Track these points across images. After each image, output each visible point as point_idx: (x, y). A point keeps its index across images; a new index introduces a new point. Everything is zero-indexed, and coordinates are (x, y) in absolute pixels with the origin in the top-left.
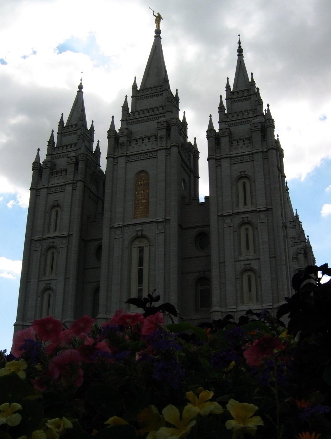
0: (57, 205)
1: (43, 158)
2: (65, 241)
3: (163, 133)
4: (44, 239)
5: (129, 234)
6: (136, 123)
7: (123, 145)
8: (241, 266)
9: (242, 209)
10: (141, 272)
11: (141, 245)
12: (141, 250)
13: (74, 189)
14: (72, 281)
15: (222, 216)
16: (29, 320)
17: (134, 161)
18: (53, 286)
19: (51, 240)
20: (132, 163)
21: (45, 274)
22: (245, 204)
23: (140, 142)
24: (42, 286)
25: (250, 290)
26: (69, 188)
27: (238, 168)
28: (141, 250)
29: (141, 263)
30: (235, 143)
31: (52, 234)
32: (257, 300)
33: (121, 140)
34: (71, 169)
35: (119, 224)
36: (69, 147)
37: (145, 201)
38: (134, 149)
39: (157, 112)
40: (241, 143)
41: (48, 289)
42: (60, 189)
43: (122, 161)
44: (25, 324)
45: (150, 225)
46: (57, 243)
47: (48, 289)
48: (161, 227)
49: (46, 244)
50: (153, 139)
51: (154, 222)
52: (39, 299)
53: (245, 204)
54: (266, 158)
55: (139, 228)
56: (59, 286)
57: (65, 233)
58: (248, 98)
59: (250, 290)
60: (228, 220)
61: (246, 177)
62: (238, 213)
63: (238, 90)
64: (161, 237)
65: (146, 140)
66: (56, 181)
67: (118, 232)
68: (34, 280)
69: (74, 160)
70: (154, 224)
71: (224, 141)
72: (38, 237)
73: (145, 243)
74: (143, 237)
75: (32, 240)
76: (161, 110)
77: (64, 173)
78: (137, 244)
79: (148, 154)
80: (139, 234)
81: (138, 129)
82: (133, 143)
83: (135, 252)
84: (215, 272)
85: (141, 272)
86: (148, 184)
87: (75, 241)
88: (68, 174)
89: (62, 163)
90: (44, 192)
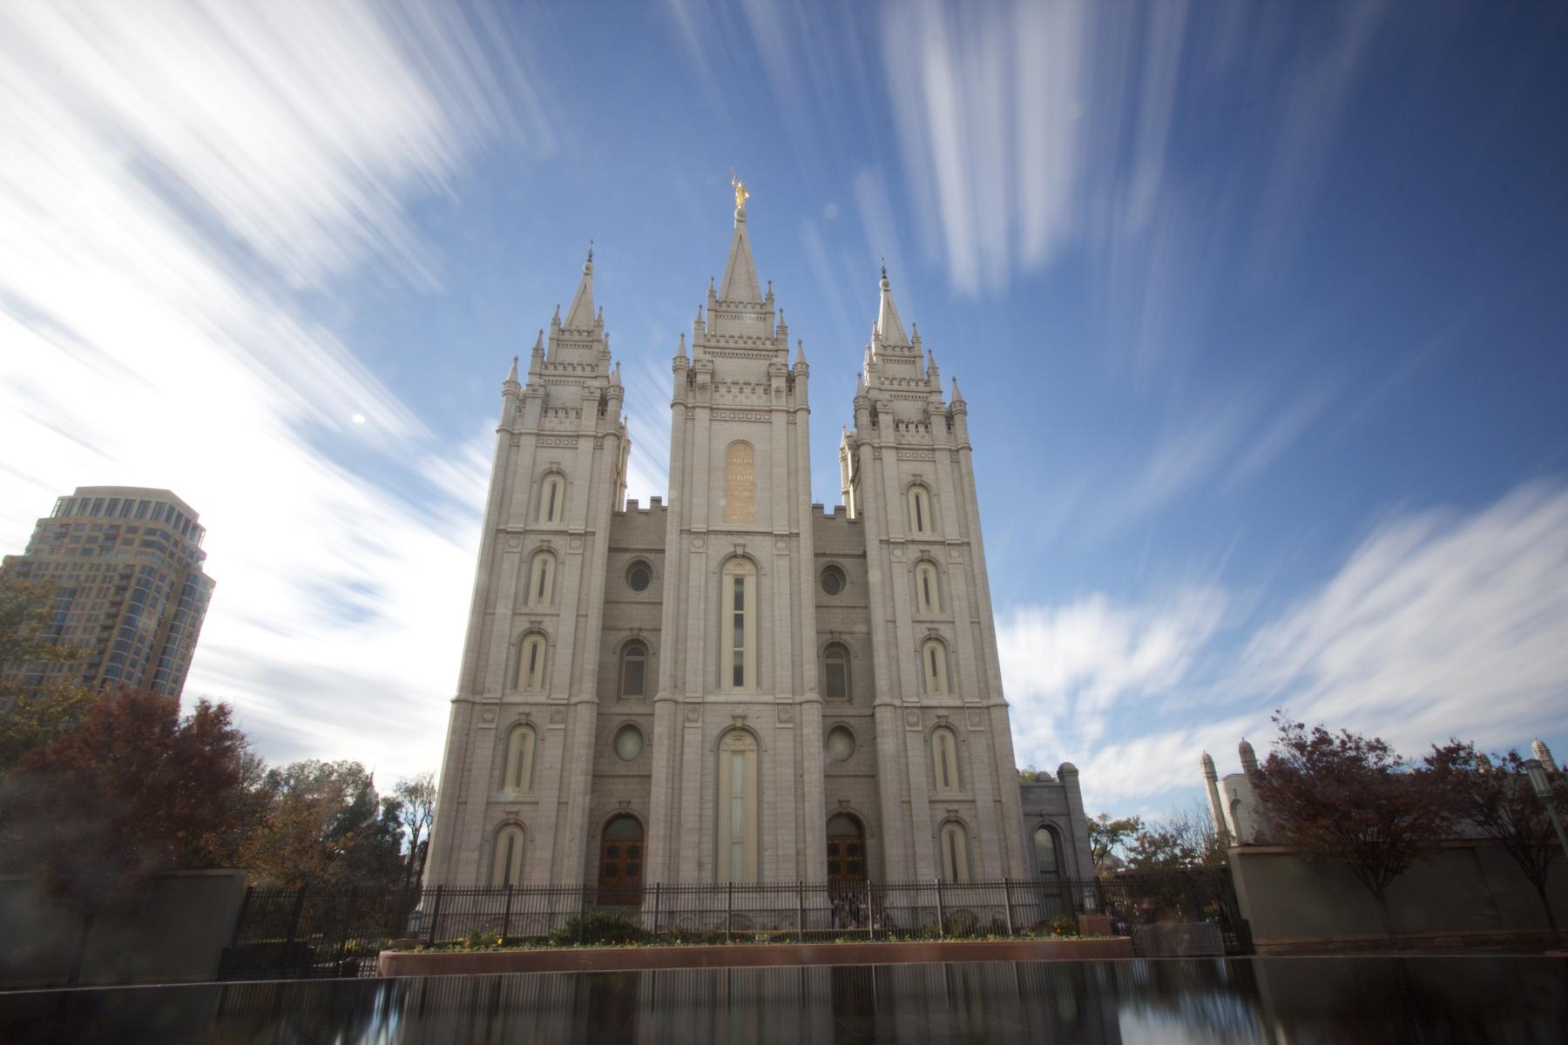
1: (524, 380)
2: (576, 543)
3: (779, 383)
4: (526, 532)
5: (722, 547)
6: (723, 355)
7: (703, 387)
8: (923, 631)
9: (917, 536)
10: (739, 621)
11: (740, 571)
12: (739, 582)
13: (599, 447)
14: (594, 622)
15: (888, 542)
18: (548, 625)
19: (544, 537)
21: (526, 602)
22: (920, 529)
24: (523, 624)
25: (935, 674)
26: (586, 446)
27: (909, 468)
28: (739, 582)
30: (902, 427)
31: (545, 525)
32: (950, 690)
33: (700, 379)
34: (591, 410)
35: (701, 527)
36: (579, 369)
37: (746, 494)
38: (725, 399)
40: (912, 427)
41: (536, 631)
43: (702, 415)
44: (478, 699)
46: (559, 543)
48: (781, 545)
49: (532, 542)
50: (760, 390)
51: (770, 534)
52: (513, 651)
53: (920, 529)
54: (955, 462)
55: (739, 540)
56: (562, 629)
57: (577, 526)
58: (913, 360)
59: (935, 674)
60: (898, 552)
61: (923, 485)
62: (913, 542)
63: (892, 343)
64: (784, 563)
65: (747, 390)
67: (698, 542)
68: (503, 609)
69: (598, 394)
71: (885, 420)
72: (516, 525)
73: (746, 569)
74: (745, 556)
75: (498, 531)
76: (768, 345)
77: (573, 414)
78: (733, 568)
80: (740, 551)
81: (728, 367)
82: (723, 390)
84: (879, 637)
86: (751, 465)
87: (600, 544)
89: (567, 394)
90: (528, 443)
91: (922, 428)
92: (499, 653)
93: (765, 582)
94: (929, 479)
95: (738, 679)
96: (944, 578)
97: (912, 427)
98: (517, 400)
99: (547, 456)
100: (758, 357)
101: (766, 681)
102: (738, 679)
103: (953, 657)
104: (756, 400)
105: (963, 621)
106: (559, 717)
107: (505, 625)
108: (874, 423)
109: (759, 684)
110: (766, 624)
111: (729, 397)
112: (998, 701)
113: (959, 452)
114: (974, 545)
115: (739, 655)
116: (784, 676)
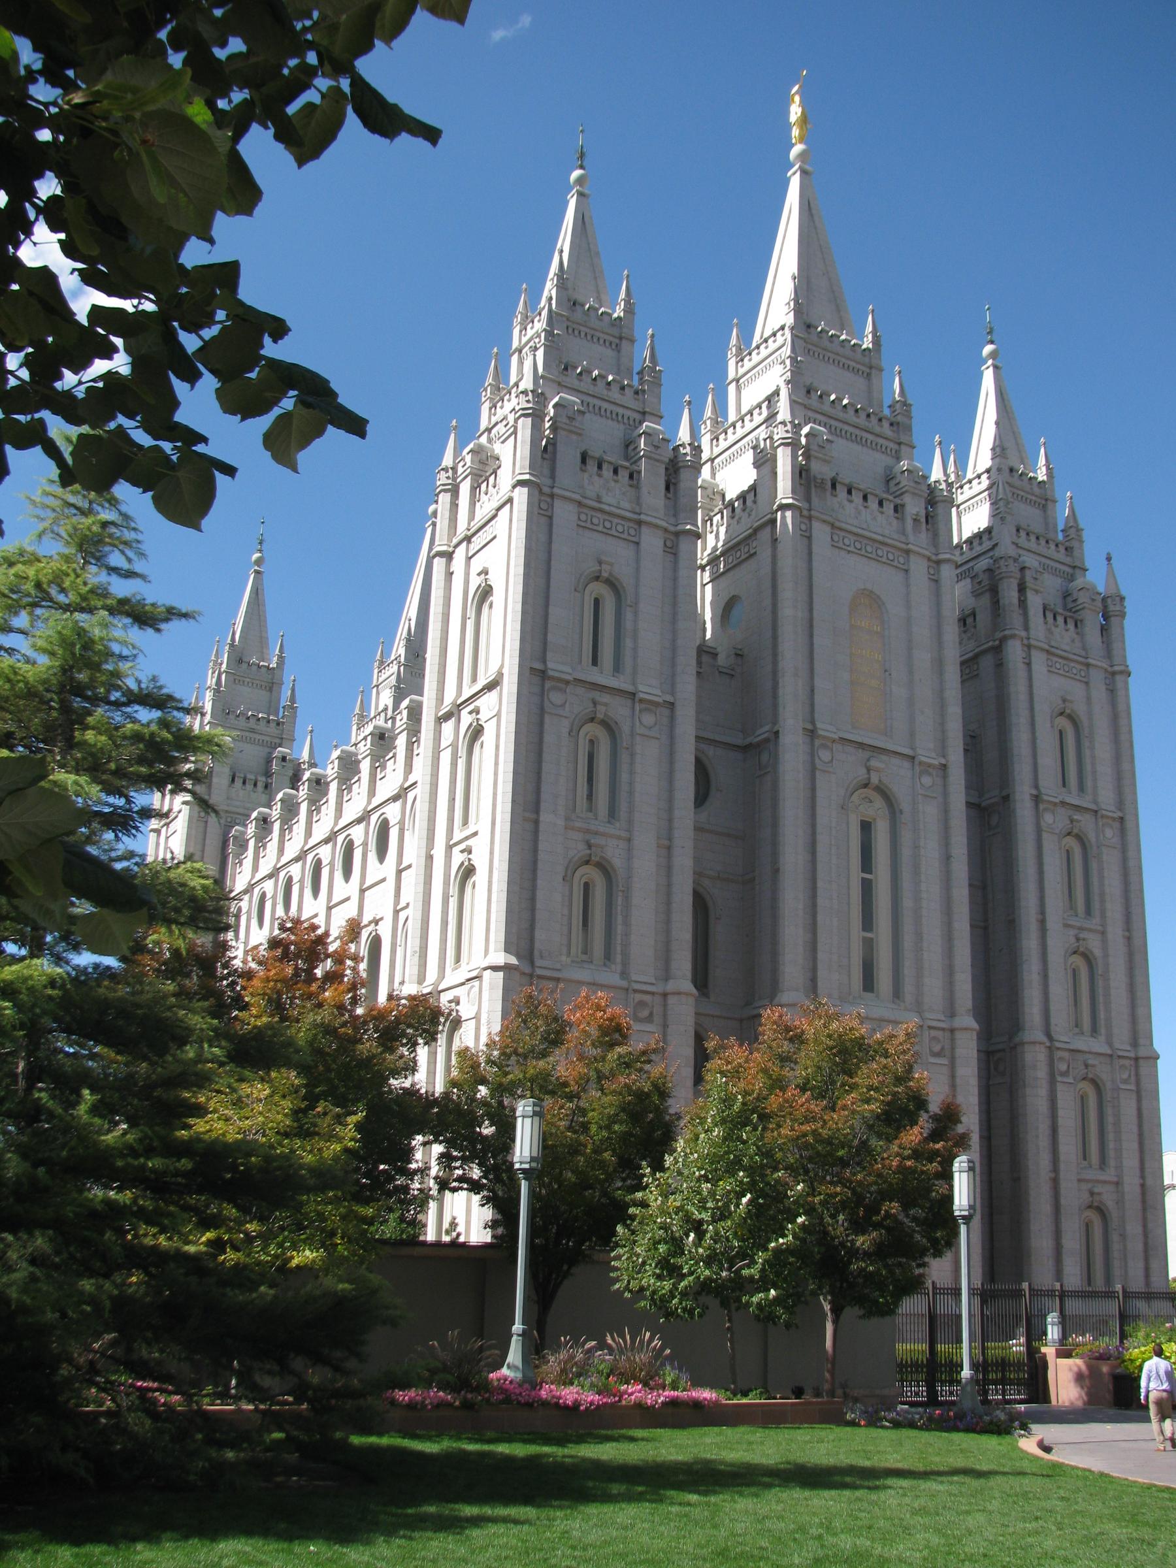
7: (821, 485)
10: (867, 888)
16: (542, 957)
17: (849, 552)
19: (596, 695)
20: (843, 553)
23: (857, 497)
39: (877, 429)
40: (1060, 620)
42: (620, 528)
43: (820, 532)
45: (896, 761)
46: (619, 710)
62: (1063, 803)
64: (930, 812)
70: (907, 764)
71: (1035, 602)
73: (876, 810)
79: (885, 549)
84: (1030, 943)
85: (867, 888)
88: (644, 490)
90: (564, 513)
91: (1071, 626)
92: (554, 896)
93: (906, 837)
94: (1080, 709)
96: (1094, 865)
97: (1060, 620)
100: (874, 447)
101: (908, 988)
103: (1100, 983)
104: (880, 522)
105: (1115, 932)
106: (646, 1013)
107: (557, 848)
108: (1023, 603)
109: (897, 994)
110: (907, 903)
111: (849, 509)
112: (1142, 1052)
113: (1117, 677)
114: (1129, 824)
116: (934, 987)
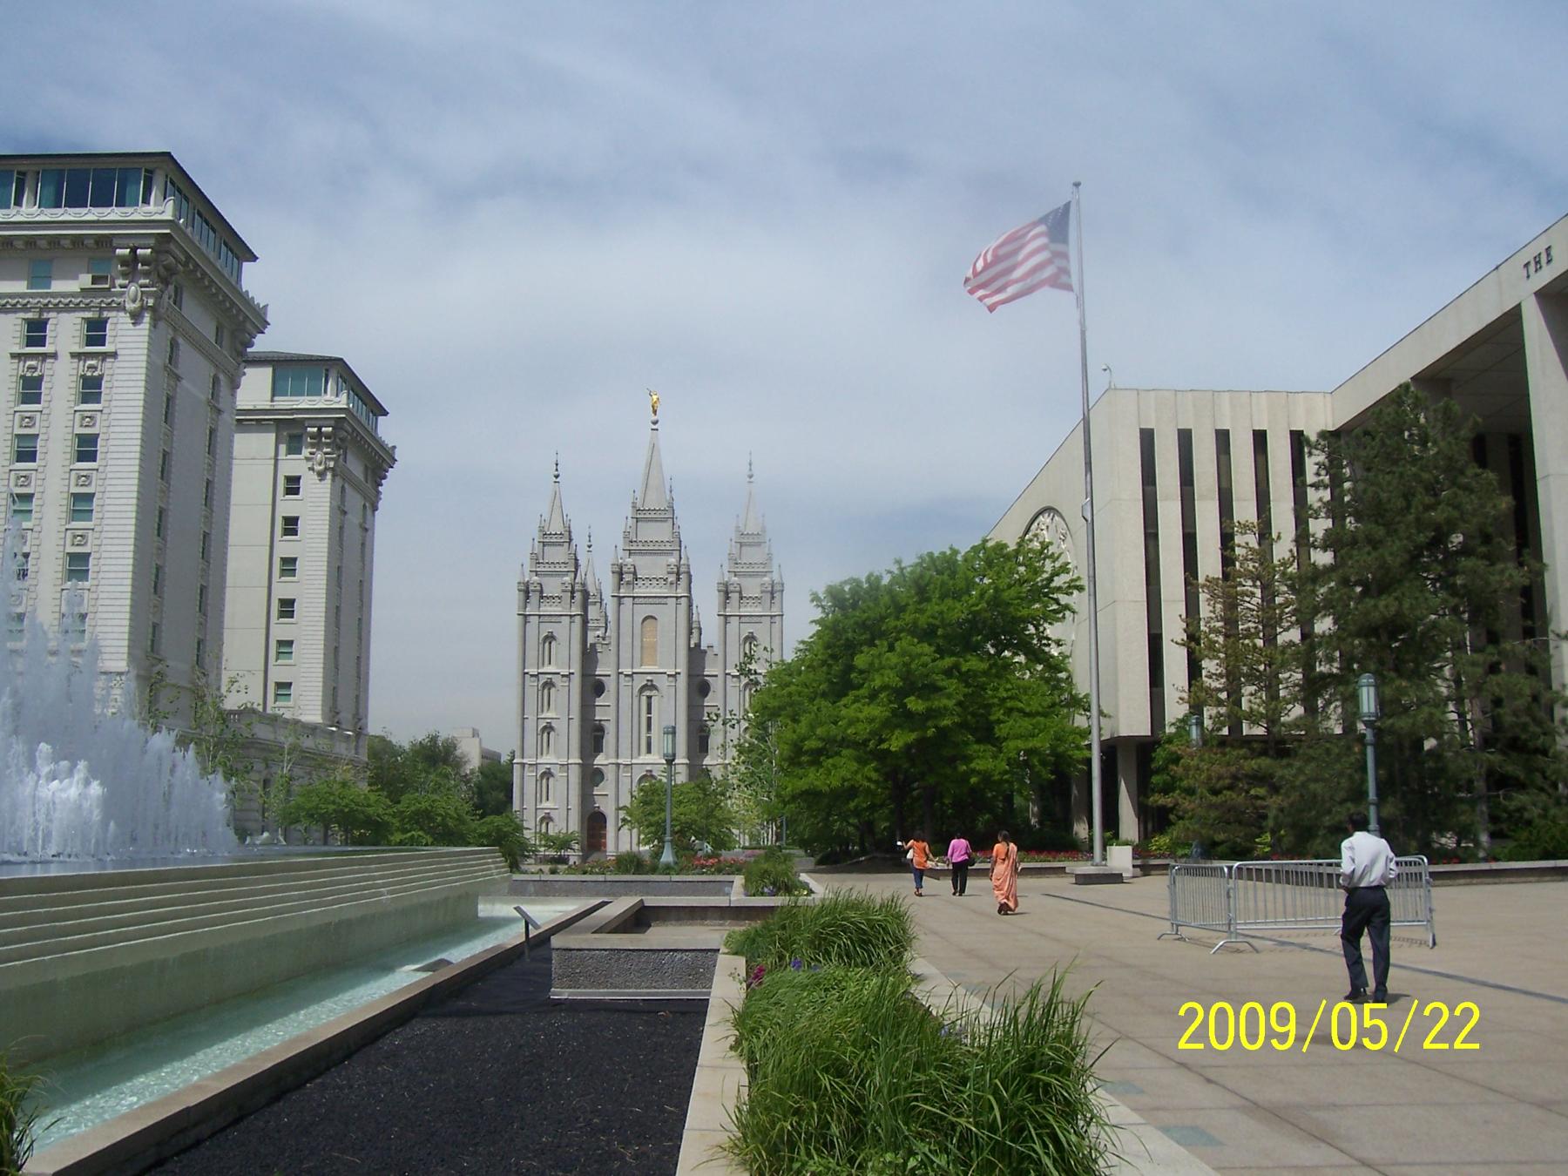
0: (550, 638)
10: (649, 719)
12: (649, 698)
27: (747, 630)
28: (649, 698)
29: (649, 712)
38: (639, 591)
41: (549, 728)
46: (556, 679)
47: (549, 728)
66: (547, 609)
78: (648, 693)
82: (640, 582)
83: (644, 699)
85: (649, 719)
87: (576, 680)
90: (534, 620)
95: (649, 751)
98: (526, 592)
99: (546, 629)
102: (649, 751)
115: (649, 739)
